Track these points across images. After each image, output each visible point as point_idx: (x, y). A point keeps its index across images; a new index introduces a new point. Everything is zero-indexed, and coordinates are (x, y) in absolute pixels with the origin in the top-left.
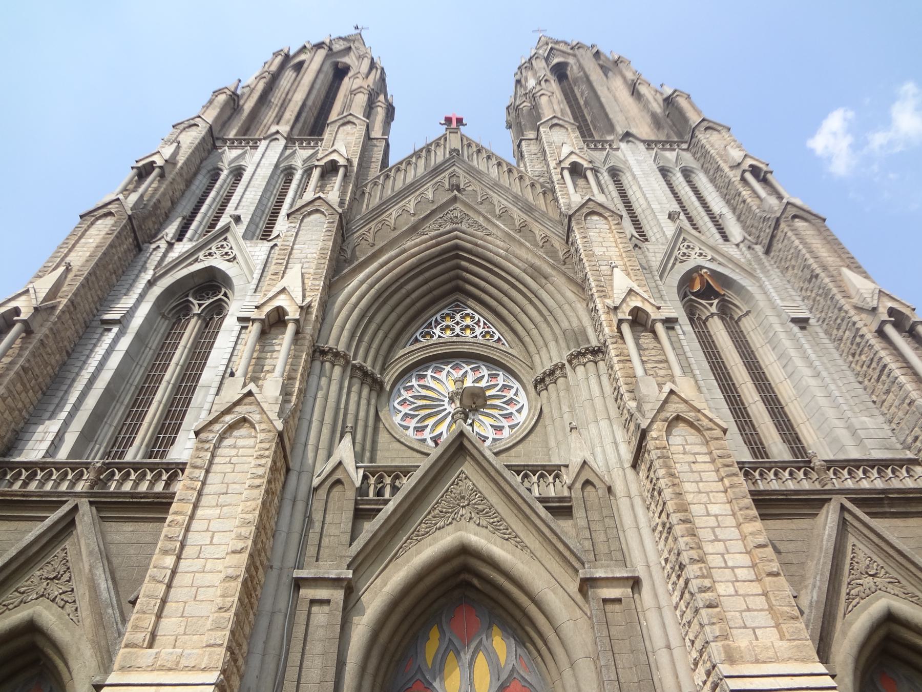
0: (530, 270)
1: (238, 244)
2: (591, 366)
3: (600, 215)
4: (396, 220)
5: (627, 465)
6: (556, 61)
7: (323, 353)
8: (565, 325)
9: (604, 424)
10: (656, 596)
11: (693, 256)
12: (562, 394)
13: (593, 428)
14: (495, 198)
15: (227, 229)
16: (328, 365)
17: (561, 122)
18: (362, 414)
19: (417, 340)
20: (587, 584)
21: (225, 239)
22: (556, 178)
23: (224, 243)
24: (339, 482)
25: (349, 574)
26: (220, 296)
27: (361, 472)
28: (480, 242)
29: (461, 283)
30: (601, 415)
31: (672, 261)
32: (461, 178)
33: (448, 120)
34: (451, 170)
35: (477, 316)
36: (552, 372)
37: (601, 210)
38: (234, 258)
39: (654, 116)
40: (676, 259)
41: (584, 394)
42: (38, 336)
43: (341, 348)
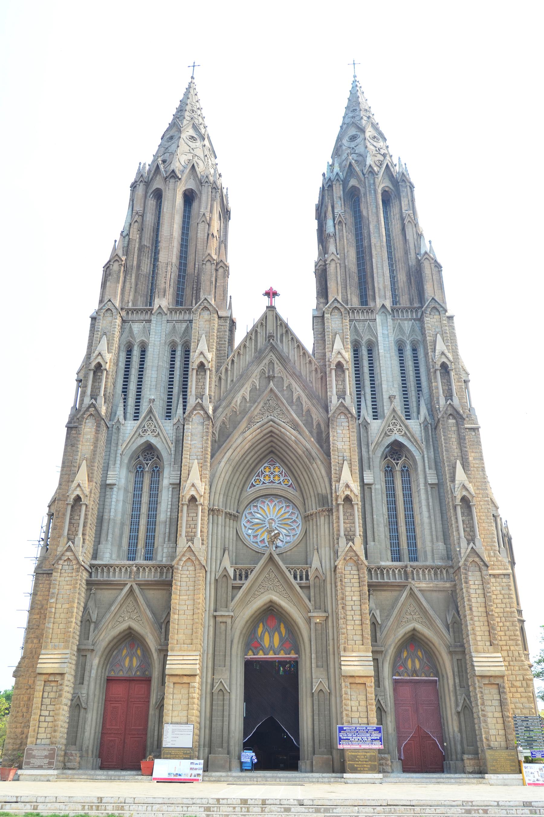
0: (306, 453)
1: (158, 423)
2: (327, 517)
3: (345, 415)
4: (240, 406)
5: (333, 570)
6: (353, 182)
7: (213, 510)
8: (319, 490)
9: (327, 549)
10: (333, 622)
11: (395, 432)
12: (315, 527)
13: (323, 549)
14: (294, 385)
15: (150, 411)
16: (215, 516)
17: (339, 306)
18: (231, 536)
19: (253, 485)
20: (310, 618)
21: (151, 418)
22: (328, 369)
23: (150, 422)
24: (225, 575)
25: (232, 614)
26: (155, 458)
27: (233, 569)
28: (283, 430)
29: (274, 450)
30: (327, 545)
31: (382, 436)
32: (276, 366)
33: (267, 294)
34: (268, 358)
35: (281, 469)
36: (311, 515)
37: (347, 412)
38: (159, 434)
39: (409, 268)
40: (386, 433)
41: (322, 531)
42: (91, 506)
43: (221, 508)
